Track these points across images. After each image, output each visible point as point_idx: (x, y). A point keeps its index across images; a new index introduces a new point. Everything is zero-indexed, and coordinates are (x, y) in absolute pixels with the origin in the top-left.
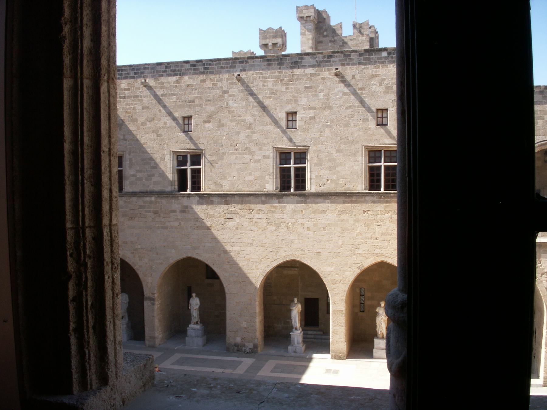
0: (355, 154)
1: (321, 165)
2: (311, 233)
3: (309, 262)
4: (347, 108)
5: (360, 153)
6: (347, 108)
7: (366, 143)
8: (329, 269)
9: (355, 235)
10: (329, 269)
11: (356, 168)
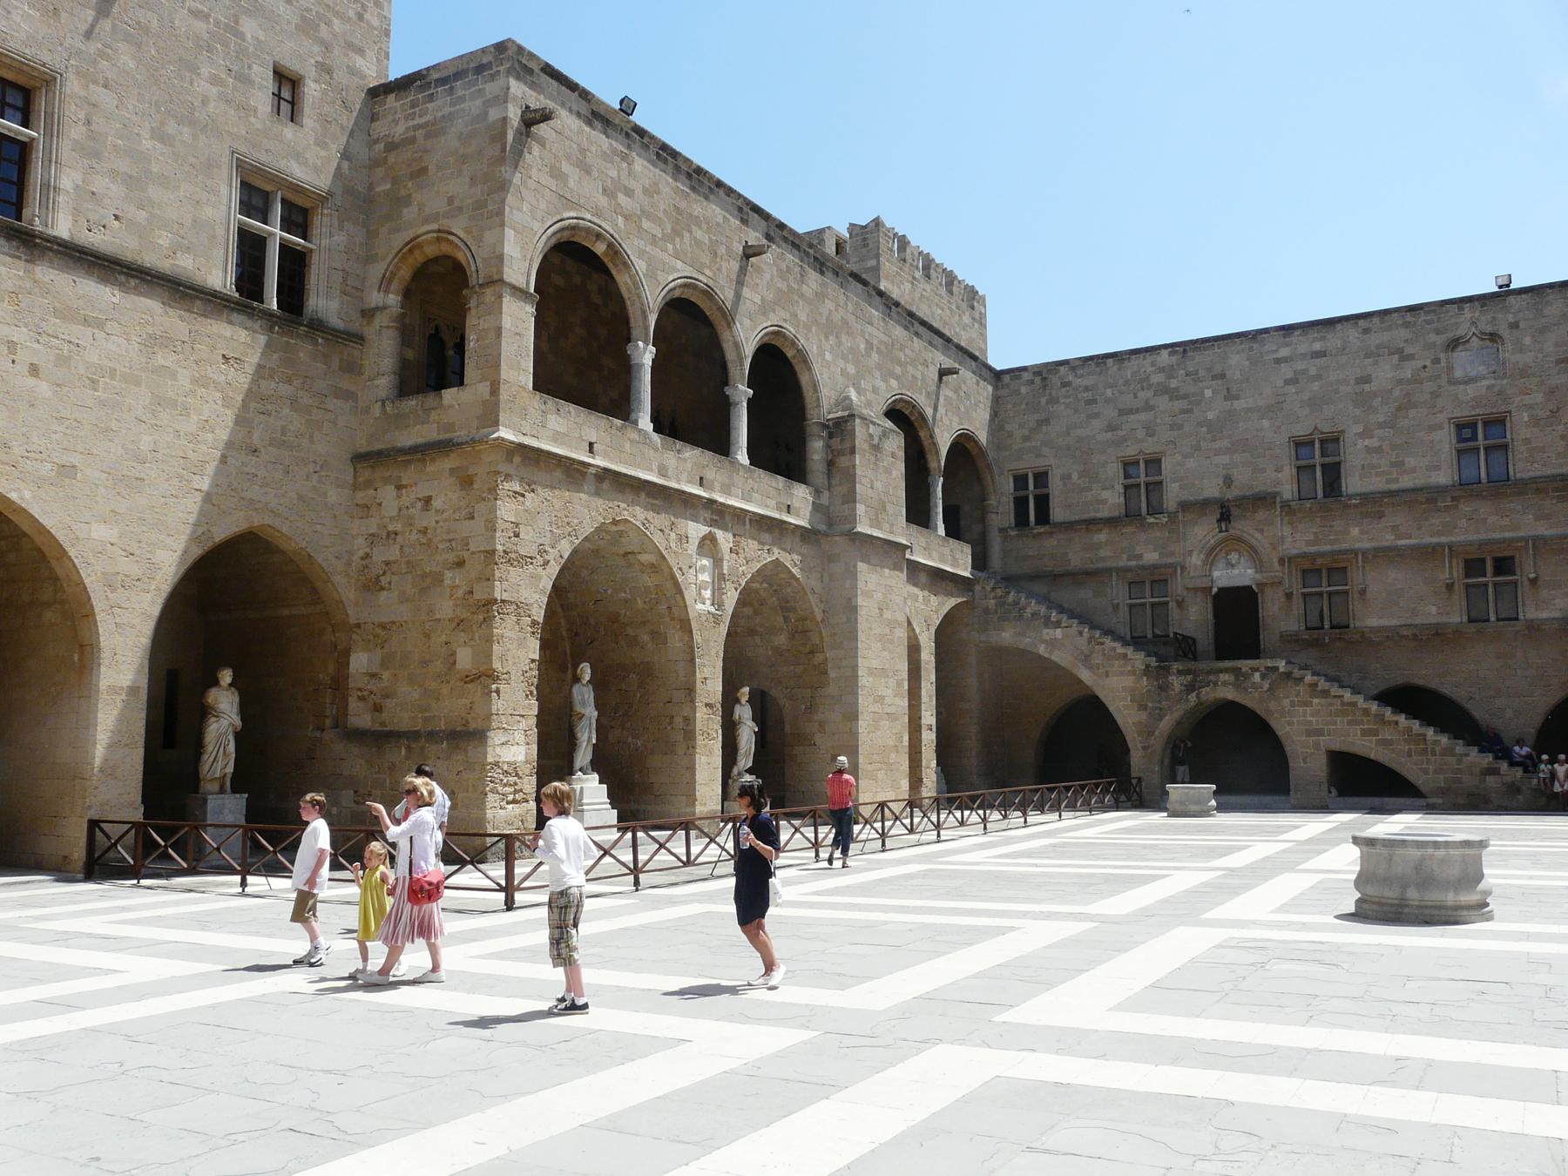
0: (209, 166)
1: (96, 155)
2: (44, 388)
3: (27, 494)
4: (195, 13)
5: (225, 171)
6: (195, 13)
7: (243, 149)
8: (100, 532)
9: (190, 425)
10: (100, 532)
11: (209, 212)
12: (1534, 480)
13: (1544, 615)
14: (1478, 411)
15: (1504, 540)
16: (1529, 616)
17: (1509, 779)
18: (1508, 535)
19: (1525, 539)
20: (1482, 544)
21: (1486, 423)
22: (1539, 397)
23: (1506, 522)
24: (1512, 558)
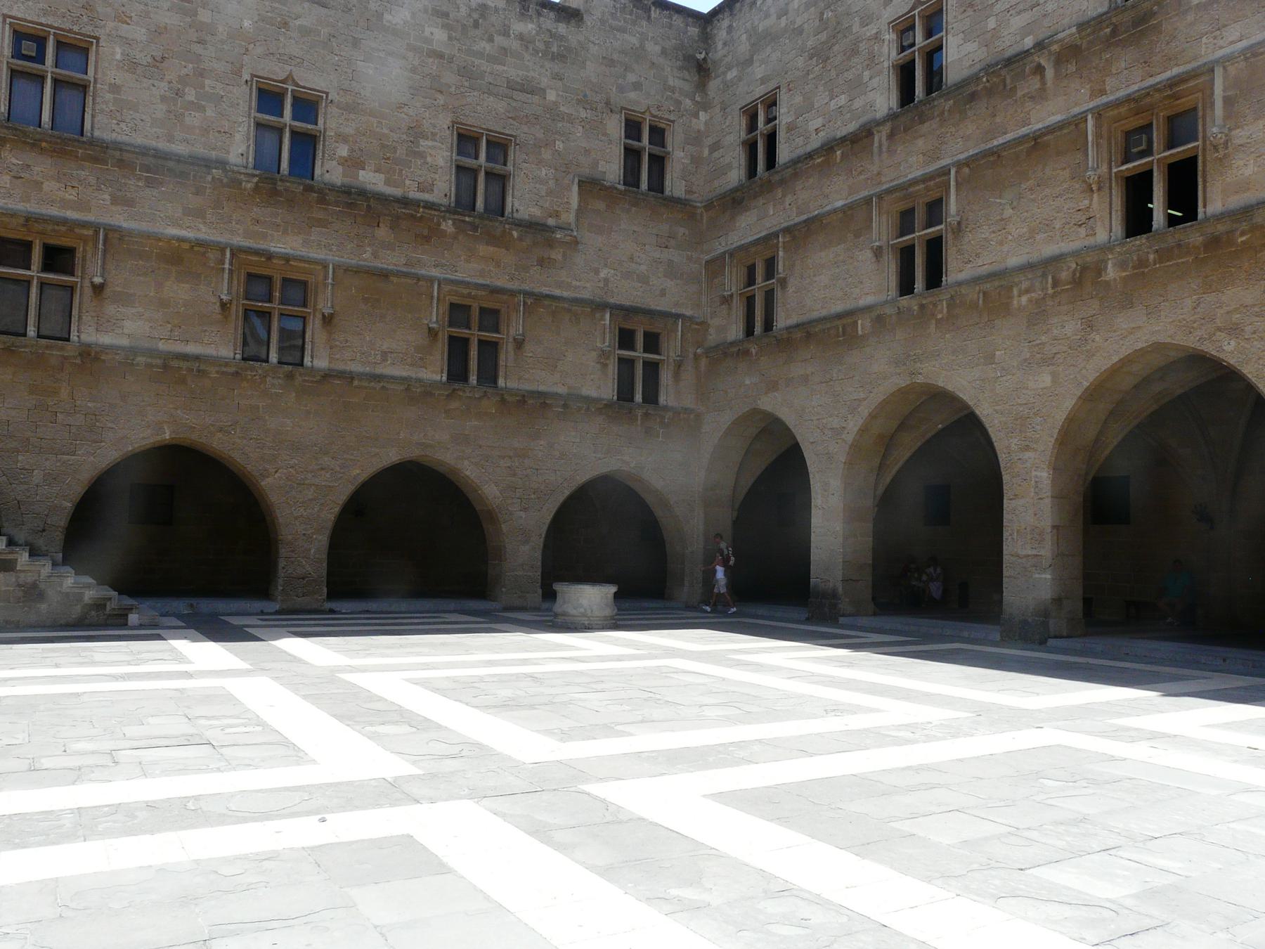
12: (118, 146)
13: (106, 339)
14: (49, 20)
15: (64, 221)
16: (85, 338)
17: (30, 578)
18: (71, 214)
19: (96, 227)
20: (29, 219)
21: (60, 45)
22: (138, 32)
23: (71, 195)
24: (71, 251)
